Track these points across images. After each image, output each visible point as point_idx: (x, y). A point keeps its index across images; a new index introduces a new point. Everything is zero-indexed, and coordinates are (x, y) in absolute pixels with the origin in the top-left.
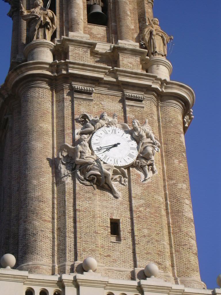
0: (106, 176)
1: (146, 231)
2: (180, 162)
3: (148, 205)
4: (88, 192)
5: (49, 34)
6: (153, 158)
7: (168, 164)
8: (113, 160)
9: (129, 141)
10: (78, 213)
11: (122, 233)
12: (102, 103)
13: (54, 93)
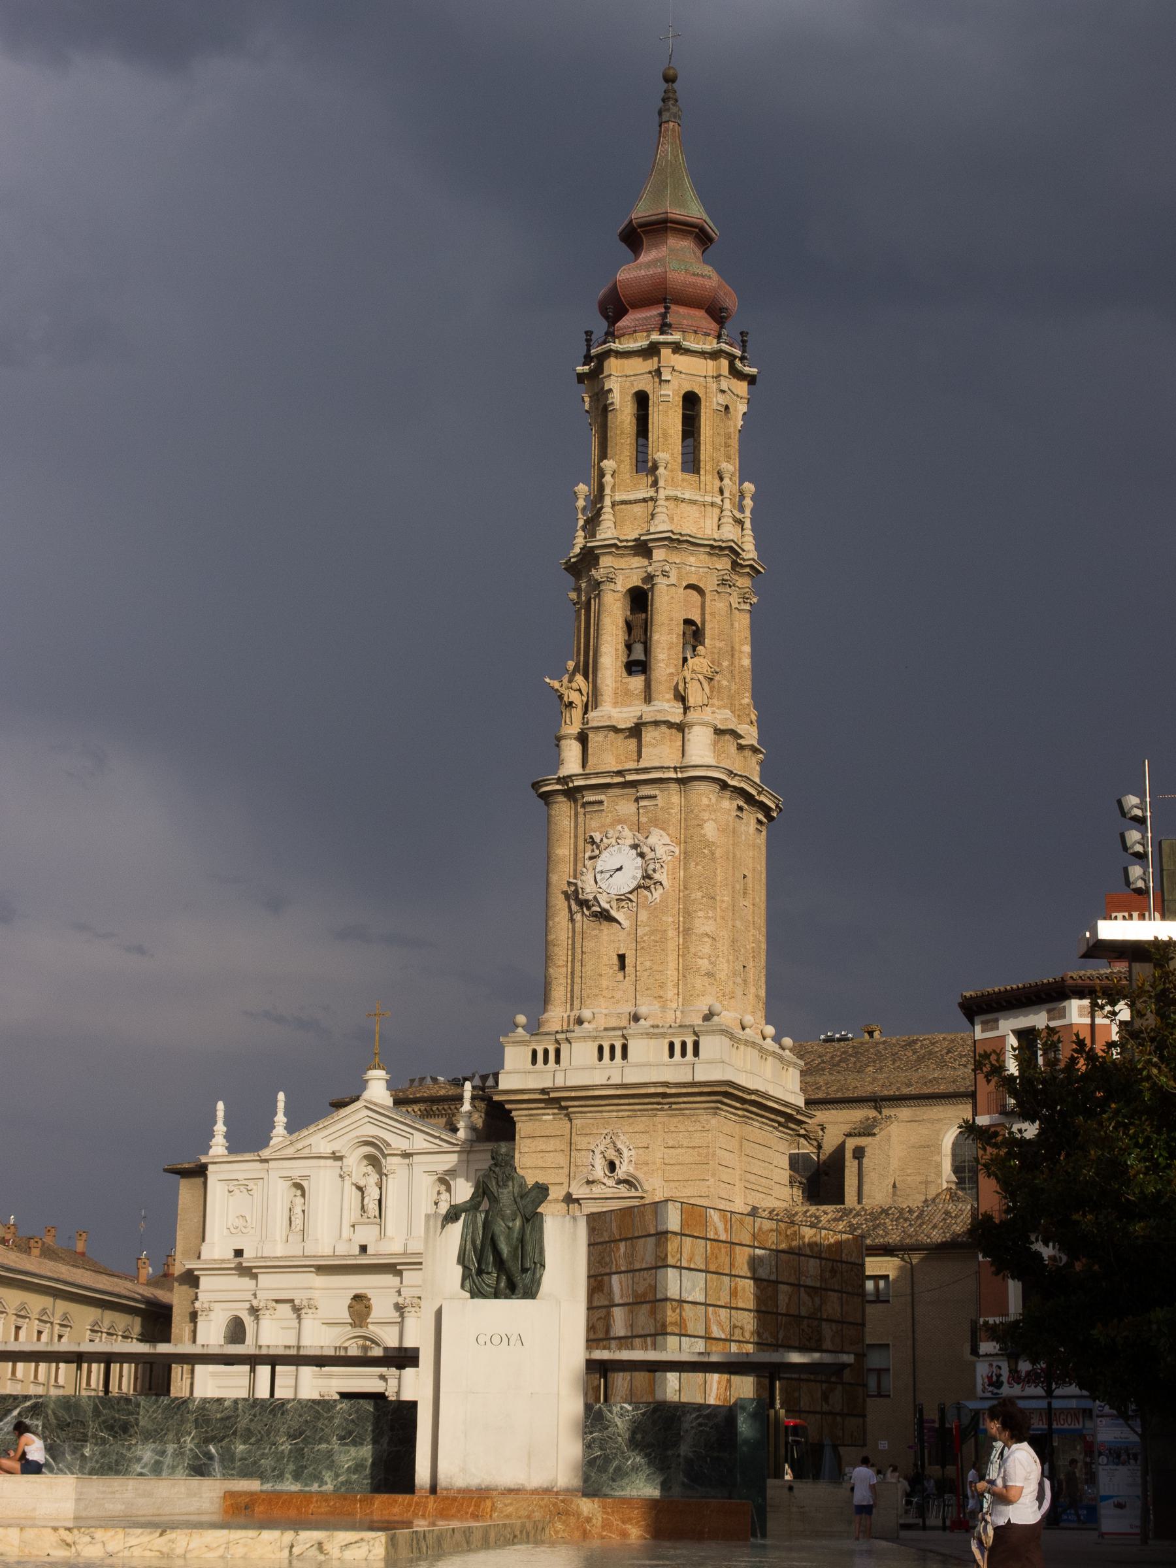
0: (607, 911)
1: (648, 964)
2: (697, 864)
3: (652, 932)
4: (595, 929)
5: (577, 713)
6: (657, 876)
7: (685, 870)
8: (616, 888)
9: (633, 860)
10: (584, 956)
11: (626, 969)
12: (616, 807)
13: (573, 805)
